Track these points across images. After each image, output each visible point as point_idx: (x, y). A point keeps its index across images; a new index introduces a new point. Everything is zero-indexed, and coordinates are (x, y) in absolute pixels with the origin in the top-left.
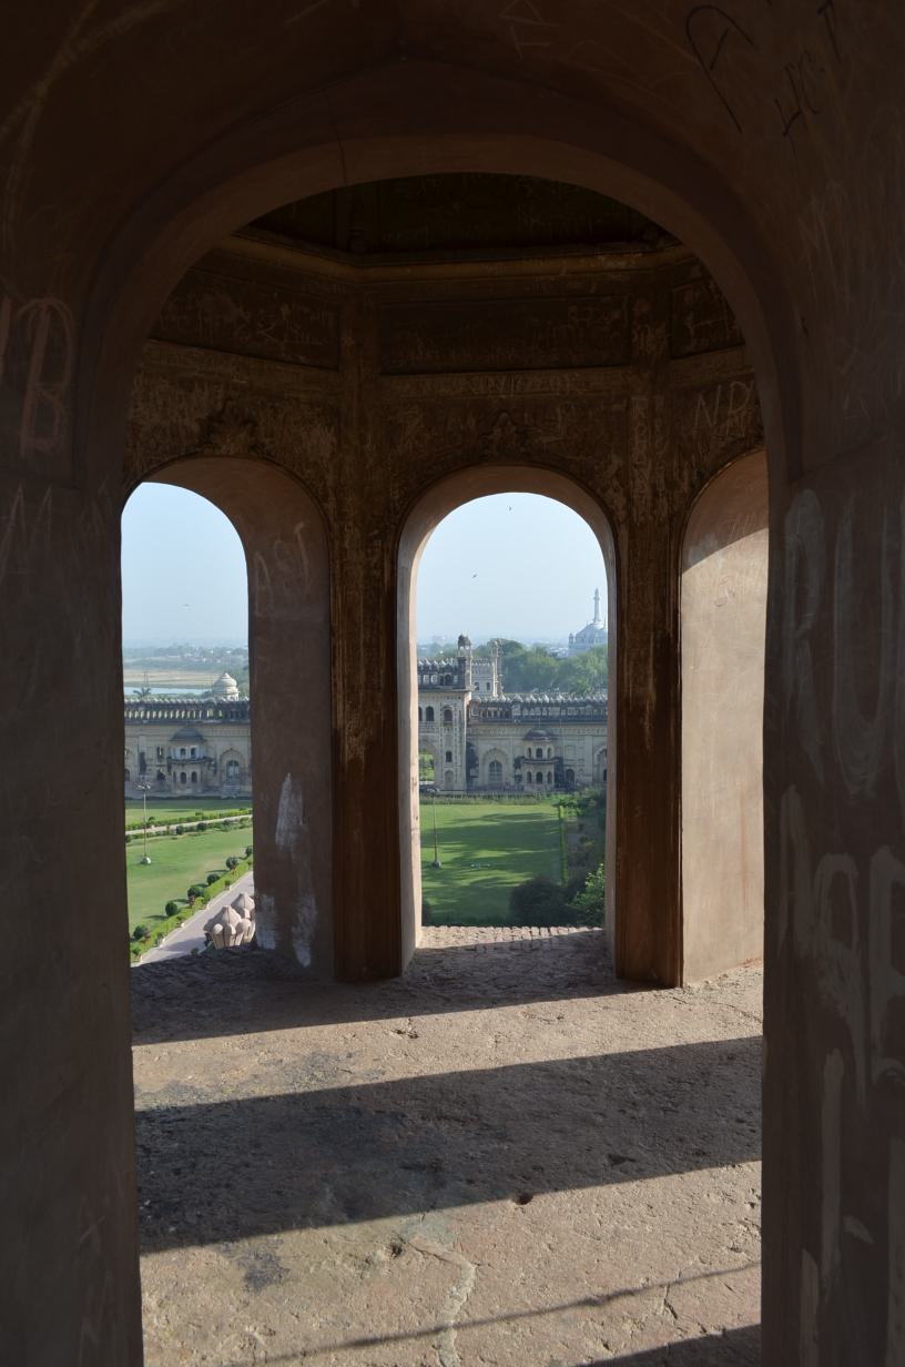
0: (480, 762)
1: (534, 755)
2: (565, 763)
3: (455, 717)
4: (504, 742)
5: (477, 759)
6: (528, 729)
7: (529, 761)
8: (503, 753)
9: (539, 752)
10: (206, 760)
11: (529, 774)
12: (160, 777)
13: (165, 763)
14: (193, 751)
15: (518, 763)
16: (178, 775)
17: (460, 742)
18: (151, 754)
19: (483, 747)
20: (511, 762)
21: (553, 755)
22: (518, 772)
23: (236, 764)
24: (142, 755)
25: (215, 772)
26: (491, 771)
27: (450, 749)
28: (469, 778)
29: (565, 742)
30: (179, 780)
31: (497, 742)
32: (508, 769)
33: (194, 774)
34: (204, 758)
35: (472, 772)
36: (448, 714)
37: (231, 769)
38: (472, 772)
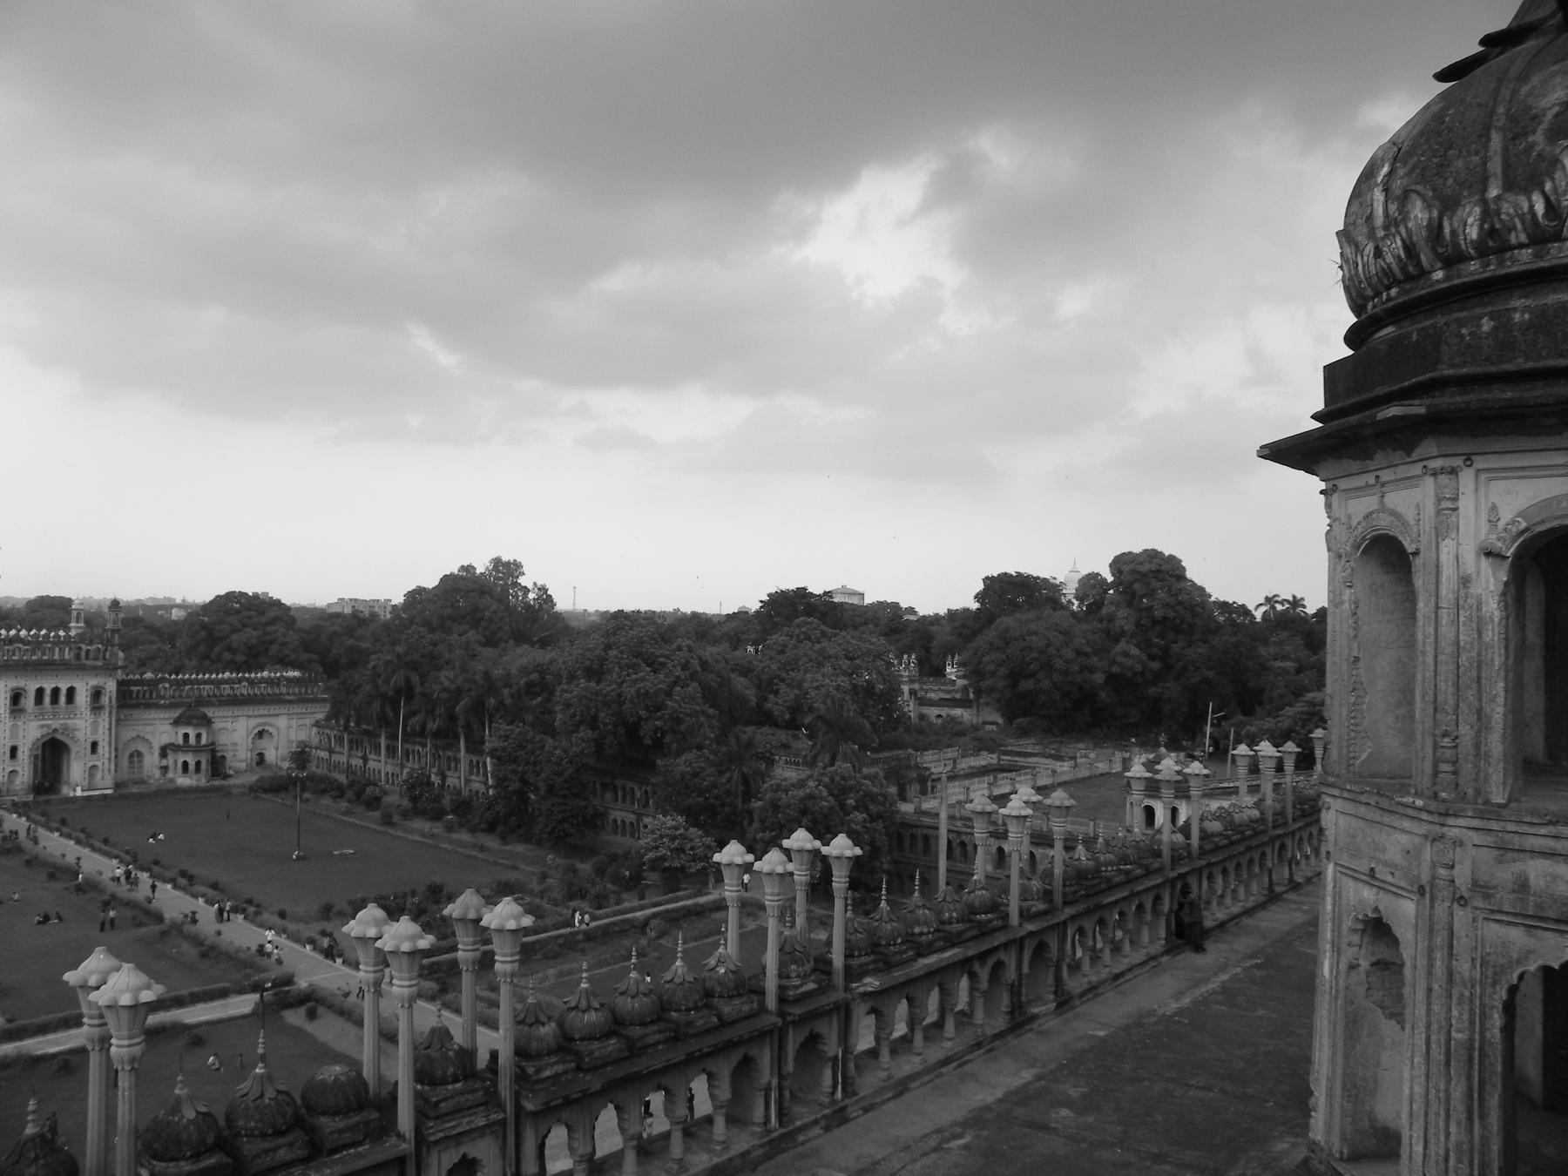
1: (192, 740)
3: (105, 700)
4: (149, 728)
6: (176, 713)
7: (185, 747)
9: (199, 736)
11: (185, 764)
15: (164, 753)
20: (157, 752)
22: (164, 762)
26: (131, 762)
29: (218, 725)
32: (151, 761)
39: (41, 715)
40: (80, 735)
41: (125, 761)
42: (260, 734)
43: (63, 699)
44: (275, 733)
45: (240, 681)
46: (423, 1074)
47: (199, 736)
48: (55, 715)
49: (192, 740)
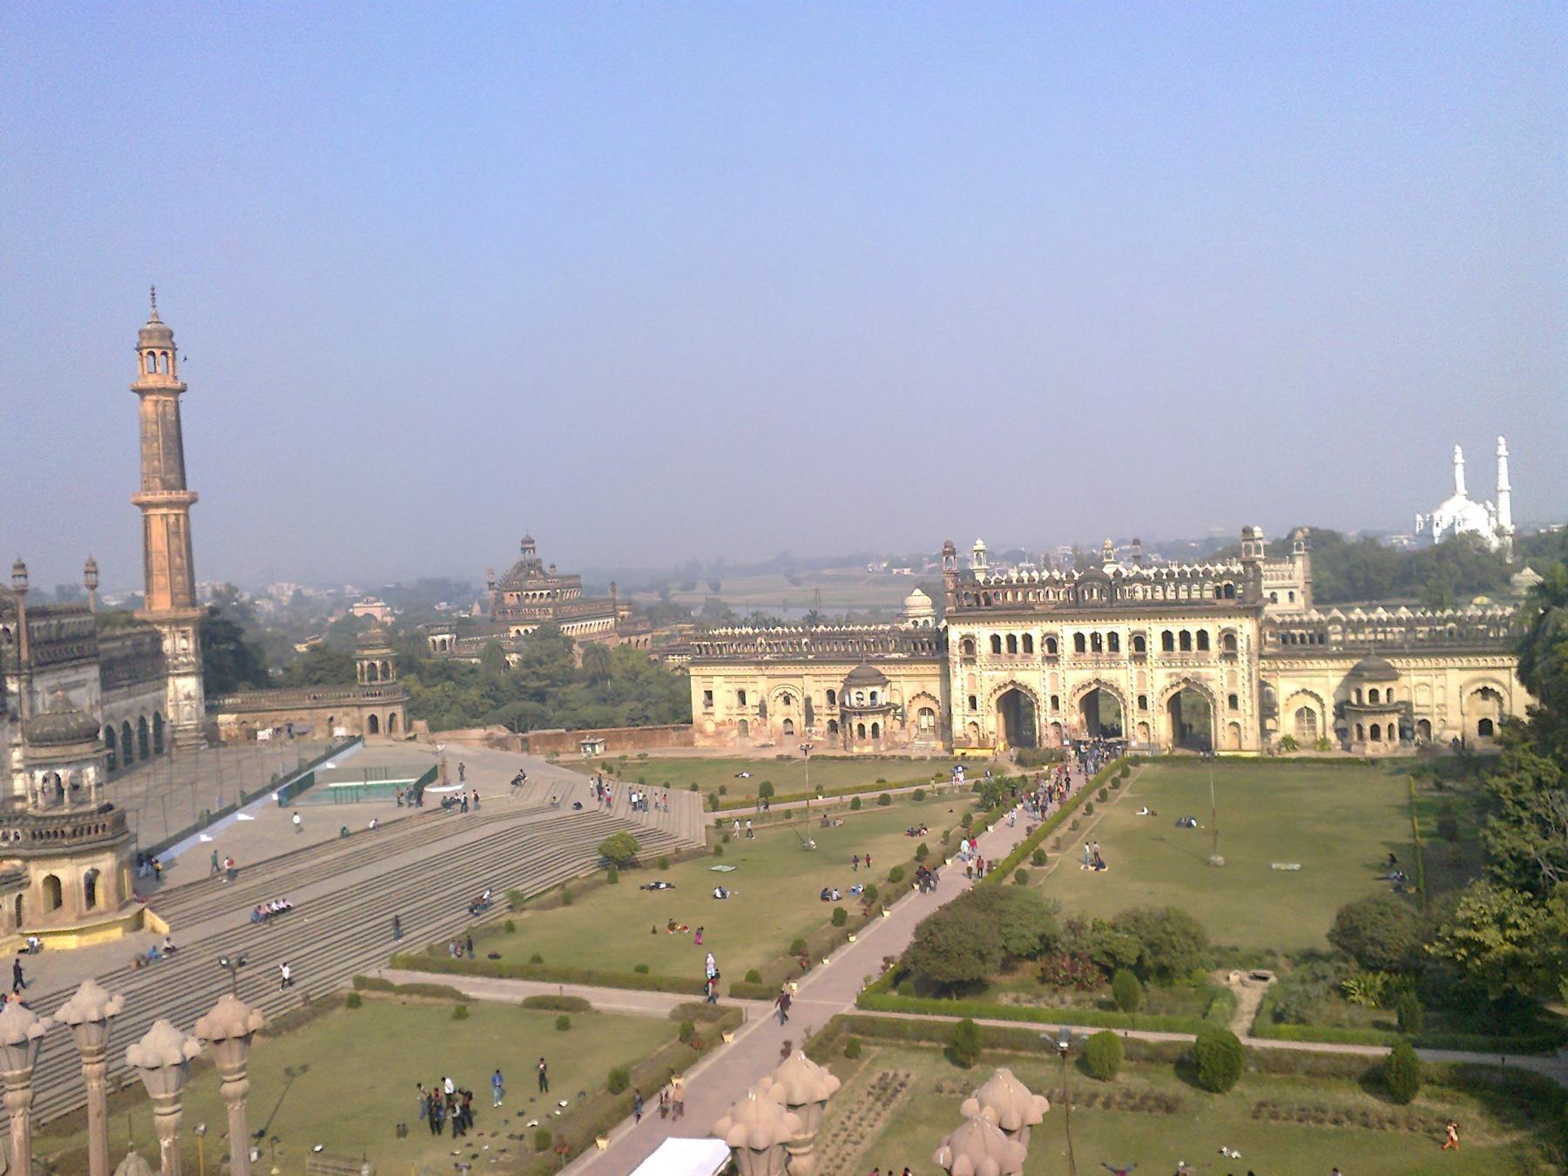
0: (1281, 708)
1: (1366, 700)
2: (1415, 710)
3: (1241, 644)
4: (1317, 681)
5: (1276, 705)
6: (1350, 664)
8: (1319, 700)
9: (1374, 693)
10: (884, 710)
13: (837, 711)
14: (873, 695)
16: (855, 727)
17: (1250, 680)
18: (820, 700)
19: (1284, 688)
21: (1396, 698)
24: (808, 700)
25: (903, 725)
27: (1233, 690)
28: (1265, 733)
30: (856, 733)
31: (1307, 680)
33: (875, 726)
35: (1270, 724)
36: (1229, 638)
37: (924, 719)
38: (1270, 724)
39: (1169, 663)
40: (1212, 686)
43: (1194, 644)
48: (1185, 663)
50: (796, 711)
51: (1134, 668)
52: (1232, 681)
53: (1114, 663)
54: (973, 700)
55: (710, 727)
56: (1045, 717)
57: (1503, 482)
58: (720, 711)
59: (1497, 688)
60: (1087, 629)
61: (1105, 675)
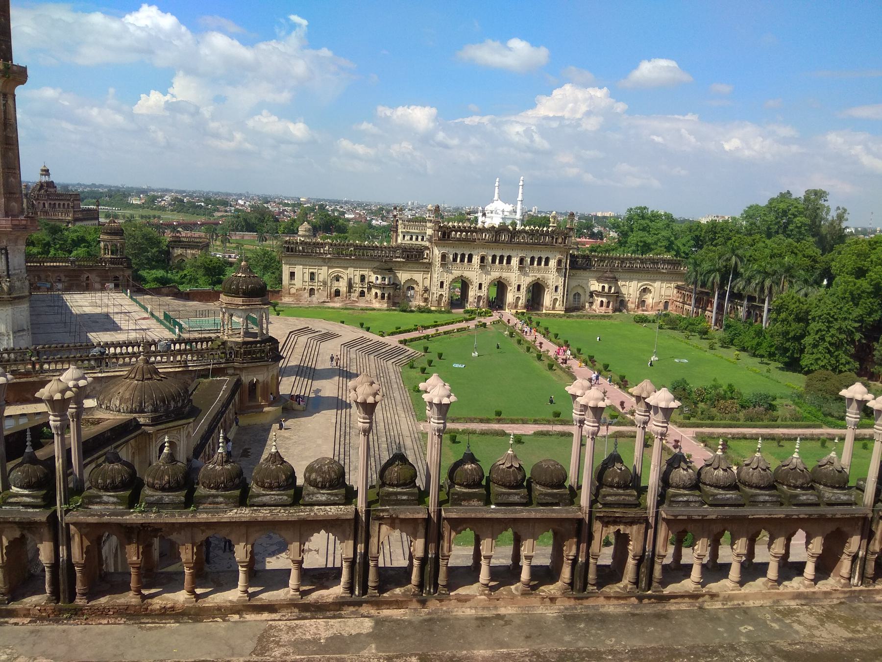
1: (606, 290)
11: (602, 302)
12: (362, 294)
18: (357, 279)
20: (588, 294)
23: (413, 288)
24: (350, 280)
30: (379, 297)
32: (585, 298)
33: (389, 294)
34: (393, 284)
40: (550, 282)
41: (571, 297)
42: (645, 290)
44: (653, 290)
45: (635, 259)
46: (600, 477)
47: (610, 288)
49: (606, 290)
50: (342, 286)
51: (518, 273)
52: (557, 281)
53: (509, 270)
54: (442, 283)
55: (293, 291)
56: (472, 293)
57: (520, 198)
58: (298, 282)
59: (650, 288)
60: (498, 254)
61: (505, 275)
